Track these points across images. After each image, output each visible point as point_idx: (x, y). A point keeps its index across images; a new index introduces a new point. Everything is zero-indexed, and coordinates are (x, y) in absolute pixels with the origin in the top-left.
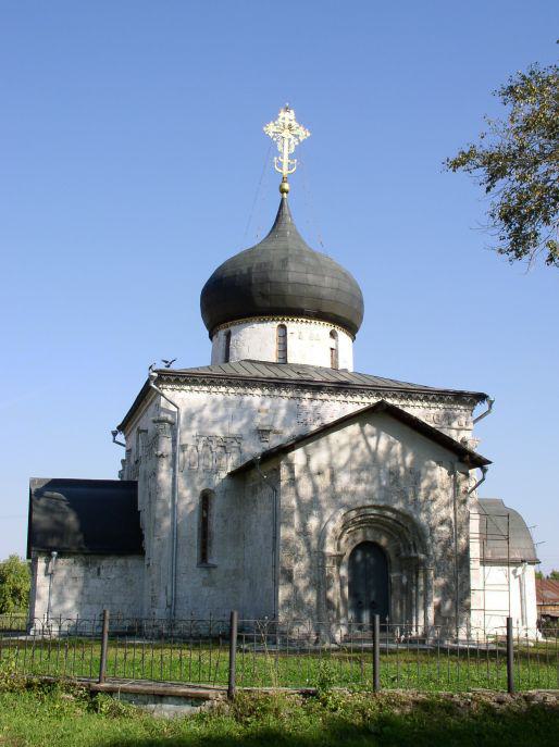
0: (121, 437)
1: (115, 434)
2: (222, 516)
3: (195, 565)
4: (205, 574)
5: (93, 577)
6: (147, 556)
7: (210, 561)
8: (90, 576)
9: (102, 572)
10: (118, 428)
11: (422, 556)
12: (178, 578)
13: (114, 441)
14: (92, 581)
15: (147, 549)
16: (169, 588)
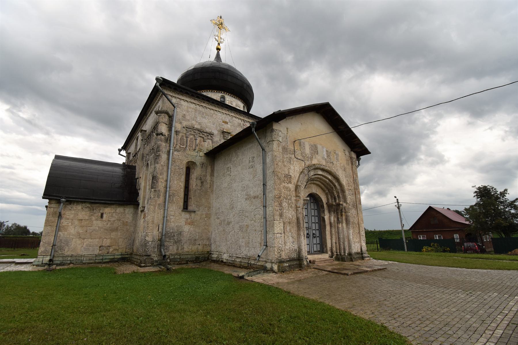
0: (123, 153)
1: (120, 150)
2: (201, 179)
3: (180, 210)
4: (187, 216)
5: (97, 220)
6: (140, 206)
7: (190, 208)
8: (93, 218)
9: (105, 216)
10: (122, 148)
11: (345, 204)
12: (168, 218)
13: (119, 154)
14: (95, 222)
15: (141, 202)
16: (161, 226)
